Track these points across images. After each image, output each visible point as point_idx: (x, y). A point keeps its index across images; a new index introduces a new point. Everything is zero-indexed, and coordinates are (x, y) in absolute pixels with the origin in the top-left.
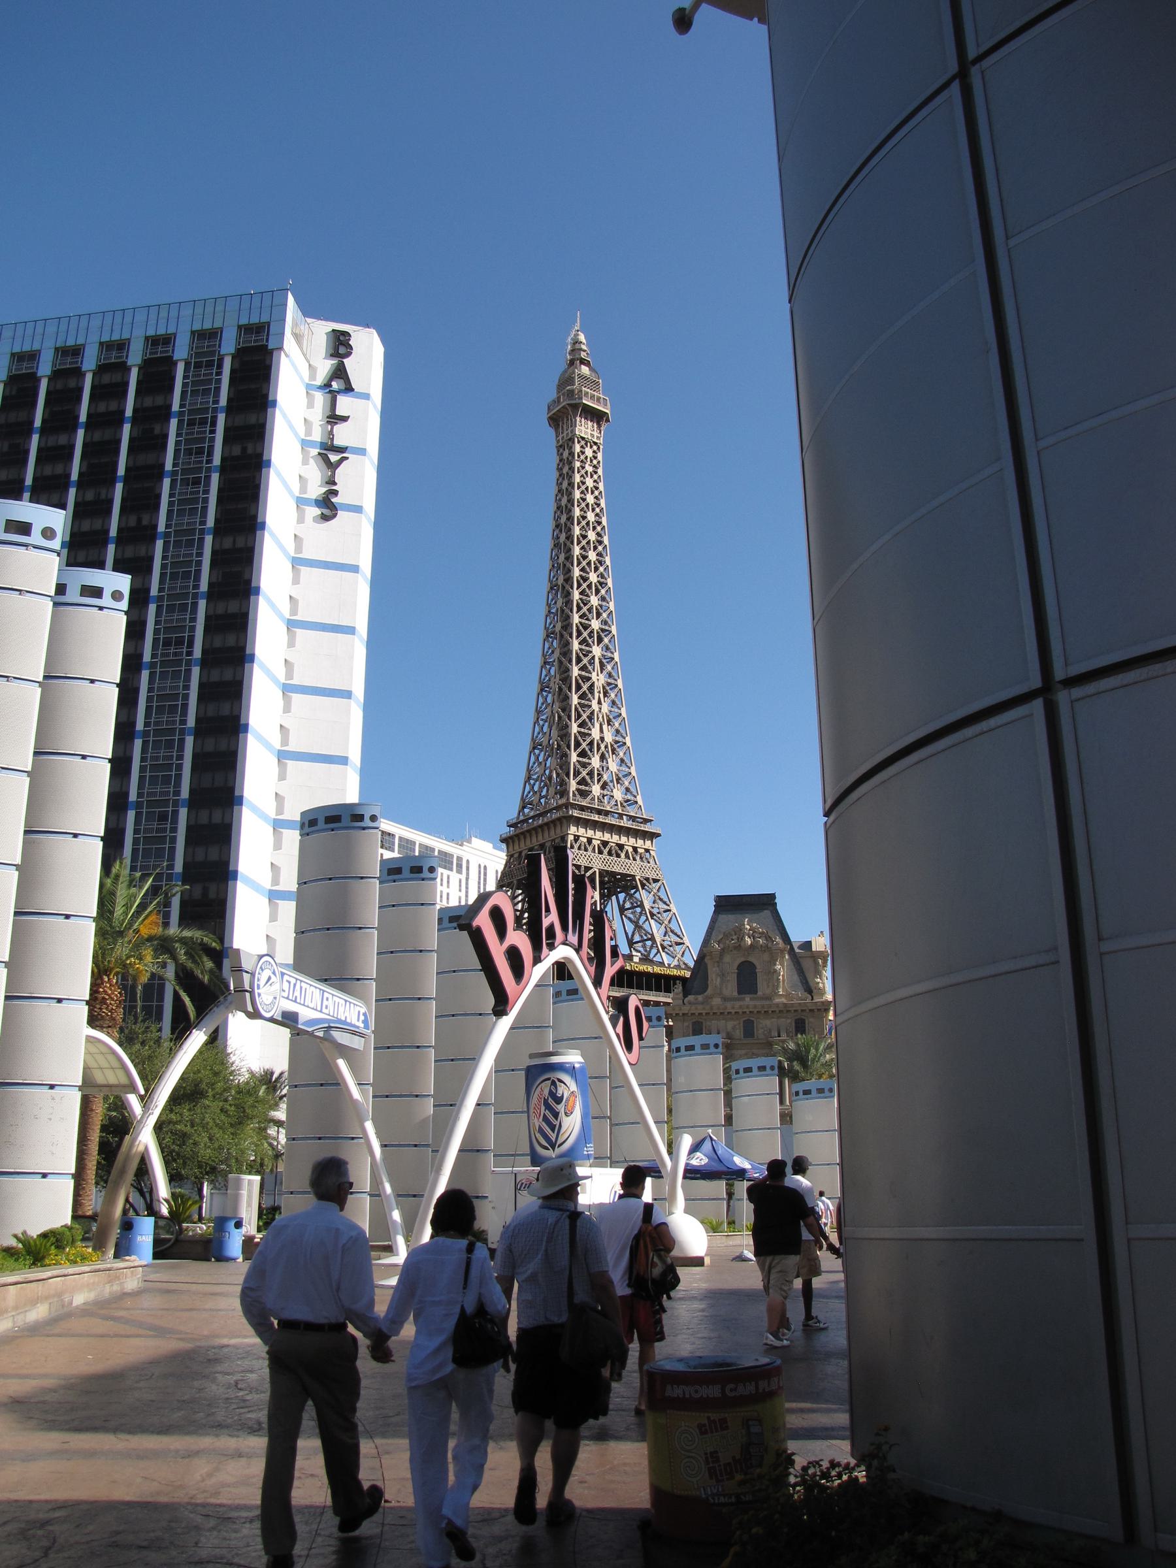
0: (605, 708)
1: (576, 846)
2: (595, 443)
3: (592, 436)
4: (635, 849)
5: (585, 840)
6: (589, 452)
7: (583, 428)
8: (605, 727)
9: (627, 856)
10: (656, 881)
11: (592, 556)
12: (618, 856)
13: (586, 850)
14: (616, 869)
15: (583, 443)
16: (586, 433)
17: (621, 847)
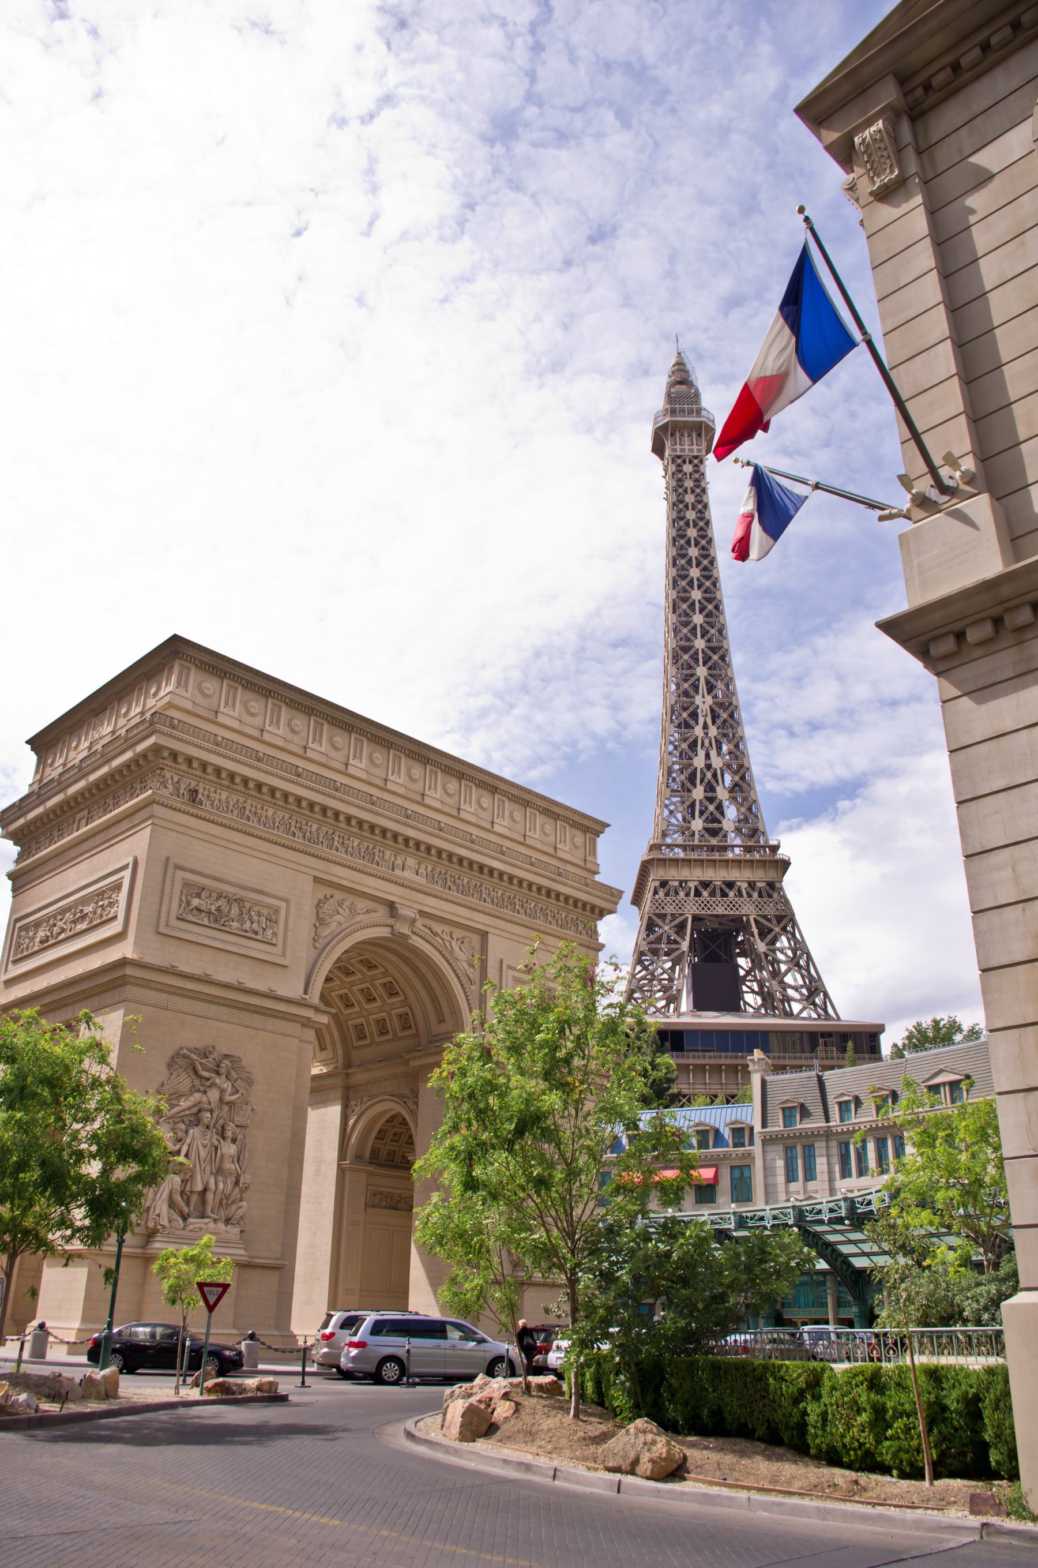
0: (713, 731)
1: (661, 893)
2: (696, 457)
3: (691, 450)
4: (752, 885)
5: (676, 884)
6: (688, 468)
7: (678, 447)
8: (713, 753)
9: (740, 894)
10: (779, 919)
11: (695, 573)
12: (724, 895)
13: (677, 893)
14: (720, 911)
15: (679, 461)
16: (683, 450)
17: (730, 885)
